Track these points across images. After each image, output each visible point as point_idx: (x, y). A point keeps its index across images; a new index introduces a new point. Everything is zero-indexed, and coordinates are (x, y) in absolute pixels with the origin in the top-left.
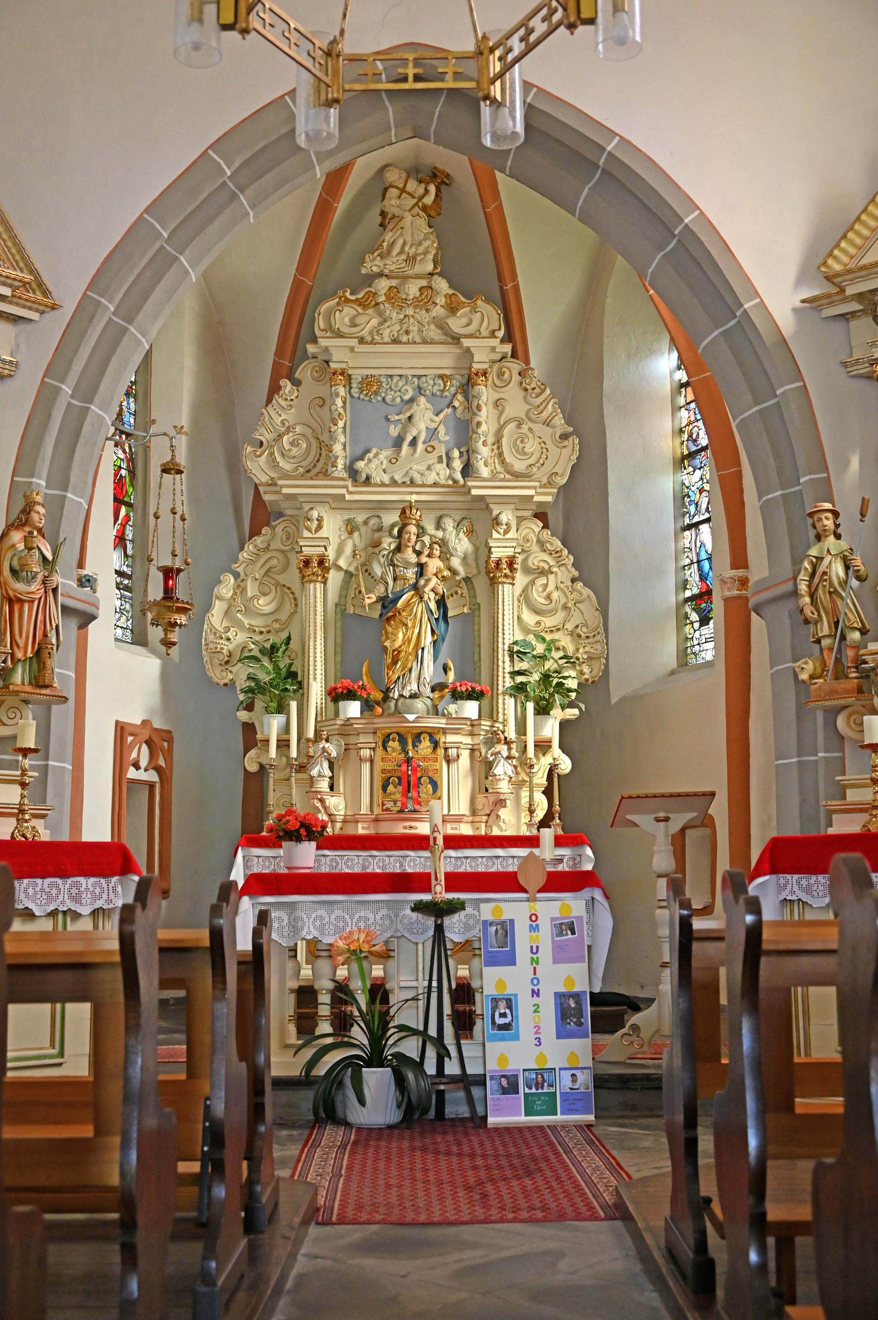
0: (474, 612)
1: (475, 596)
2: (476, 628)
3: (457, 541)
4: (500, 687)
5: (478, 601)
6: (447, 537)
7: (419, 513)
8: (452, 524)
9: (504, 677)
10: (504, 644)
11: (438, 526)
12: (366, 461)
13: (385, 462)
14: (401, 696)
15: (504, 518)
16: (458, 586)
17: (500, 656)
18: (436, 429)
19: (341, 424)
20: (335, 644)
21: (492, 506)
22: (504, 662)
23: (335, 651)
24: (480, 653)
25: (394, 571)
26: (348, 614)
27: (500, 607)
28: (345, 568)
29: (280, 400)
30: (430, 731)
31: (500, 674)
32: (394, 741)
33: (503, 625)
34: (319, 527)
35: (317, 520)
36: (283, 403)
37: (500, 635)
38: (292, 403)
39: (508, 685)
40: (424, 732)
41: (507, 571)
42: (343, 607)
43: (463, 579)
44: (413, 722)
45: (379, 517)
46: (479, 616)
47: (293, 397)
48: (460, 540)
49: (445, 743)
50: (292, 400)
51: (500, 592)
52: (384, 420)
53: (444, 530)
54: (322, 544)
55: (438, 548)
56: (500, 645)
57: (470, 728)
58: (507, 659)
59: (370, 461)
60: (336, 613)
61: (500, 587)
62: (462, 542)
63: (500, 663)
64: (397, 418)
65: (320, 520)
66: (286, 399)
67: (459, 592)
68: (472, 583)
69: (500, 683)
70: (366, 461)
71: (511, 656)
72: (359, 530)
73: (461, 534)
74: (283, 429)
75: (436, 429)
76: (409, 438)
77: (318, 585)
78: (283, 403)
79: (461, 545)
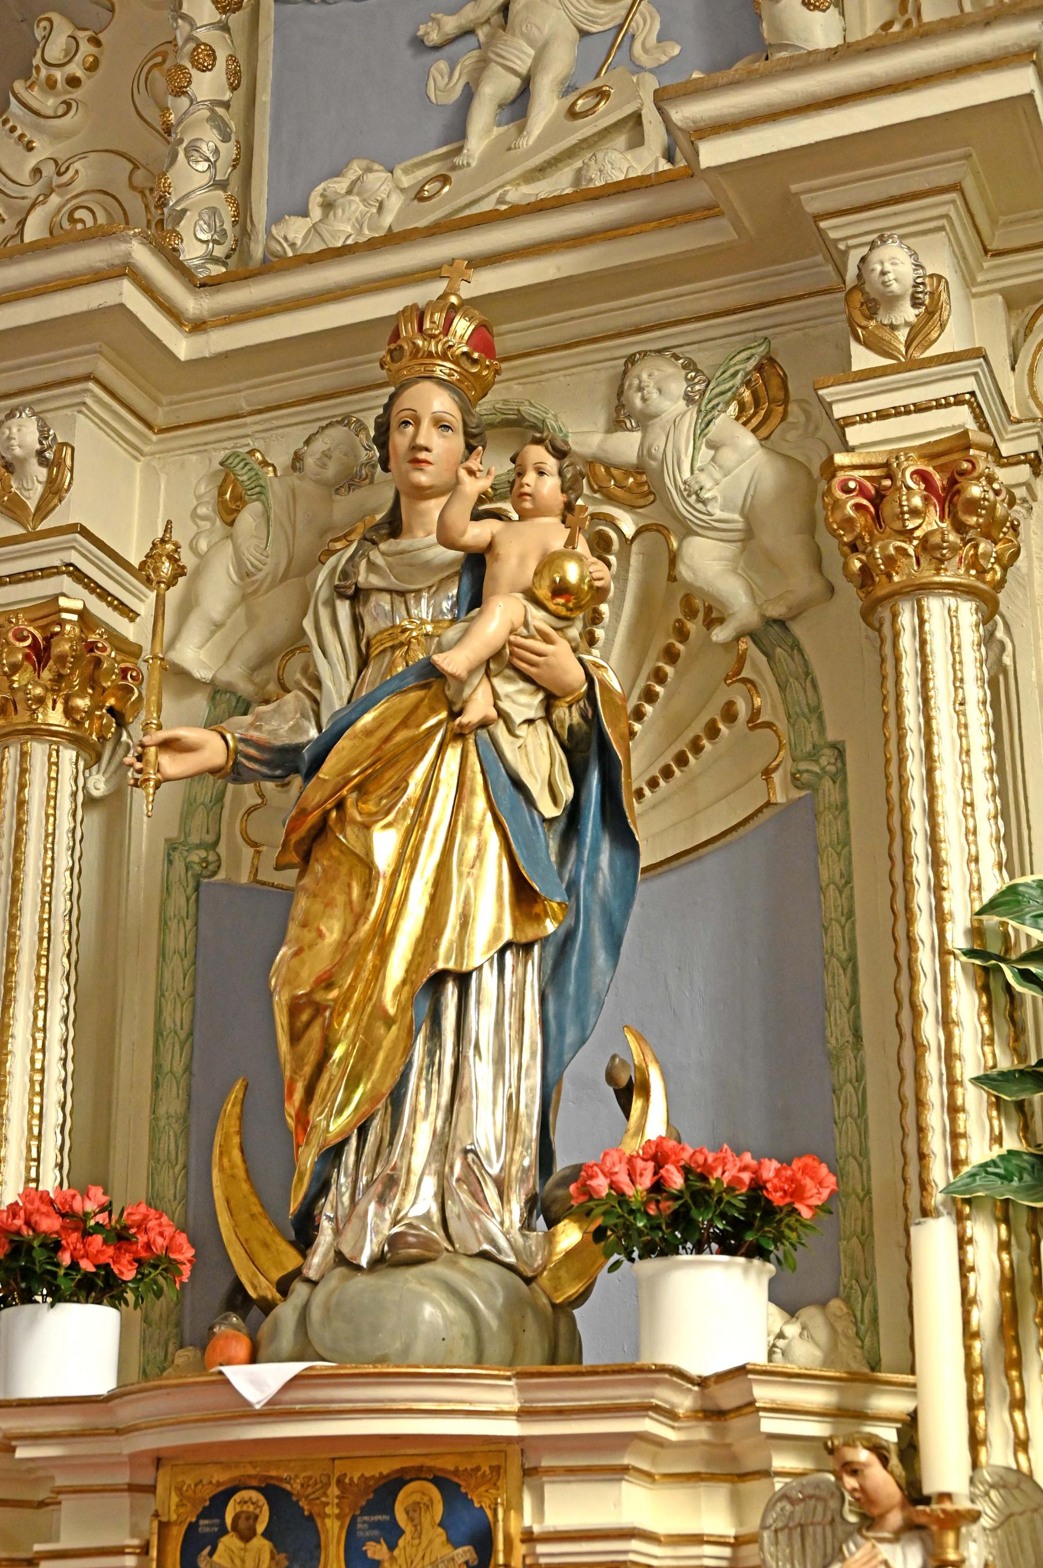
0: (814, 788)
1: (816, 712)
2: (829, 870)
3: (705, 454)
4: (939, 1173)
5: (831, 736)
6: (658, 445)
7: (462, 327)
8: (678, 387)
9: (953, 1110)
10: (940, 917)
11: (622, 415)
12: (316, 213)
13: (395, 203)
14: (341, 1260)
15: (896, 265)
16: (734, 675)
17: (927, 993)
18: (621, 26)
19: (207, 85)
20: (158, 1034)
21: (835, 229)
22: (946, 1022)
23: (157, 1067)
24: (855, 1001)
25: (357, 622)
26: (228, 885)
27: (912, 720)
28: (202, 673)
29: (35, 97)
30: (447, 1464)
31: (934, 1093)
32: (246, 1537)
33: (931, 815)
34: (54, 491)
35: (43, 461)
36: (49, 104)
37: (921, 871)
38: (77, 94)
39: (978, 1151)
40: (417, 1474)
41: (932, 522)
42: (195, 857)
43: (753, 635)
44: (276, 1410)
45: (345, 420)
46: (844, 806)
47: (75, 68)
48: (713, 446)
49: (529, 1537)
50: (73, 82)
51: (907, 643)
52: (408, 53)
53: (644, 420)
54: (54, 560)
55: (551, 463)
56: (924, 928)
57: (702, 1433)
58: (966, 1001)
59: (328, 206)
60: (167, 889)
61: (906, 619)
62: (727, 456)
63: (930, 1030)
64: (451, 24)
65: (54, 458)
66: (51, 84)
67: (742, 708)
68: (796, 646)
69: (937, 1144)
70: (316, 213)
71: (987, 980)
72: (261, 493)
73: (725, 422)
74: (32, 193)
75: (621, 26)
76: (500, 84)
77: (38, 750)
78: (49, 104)
79: (725, 466)
